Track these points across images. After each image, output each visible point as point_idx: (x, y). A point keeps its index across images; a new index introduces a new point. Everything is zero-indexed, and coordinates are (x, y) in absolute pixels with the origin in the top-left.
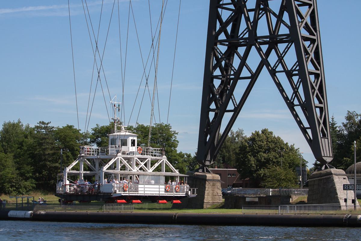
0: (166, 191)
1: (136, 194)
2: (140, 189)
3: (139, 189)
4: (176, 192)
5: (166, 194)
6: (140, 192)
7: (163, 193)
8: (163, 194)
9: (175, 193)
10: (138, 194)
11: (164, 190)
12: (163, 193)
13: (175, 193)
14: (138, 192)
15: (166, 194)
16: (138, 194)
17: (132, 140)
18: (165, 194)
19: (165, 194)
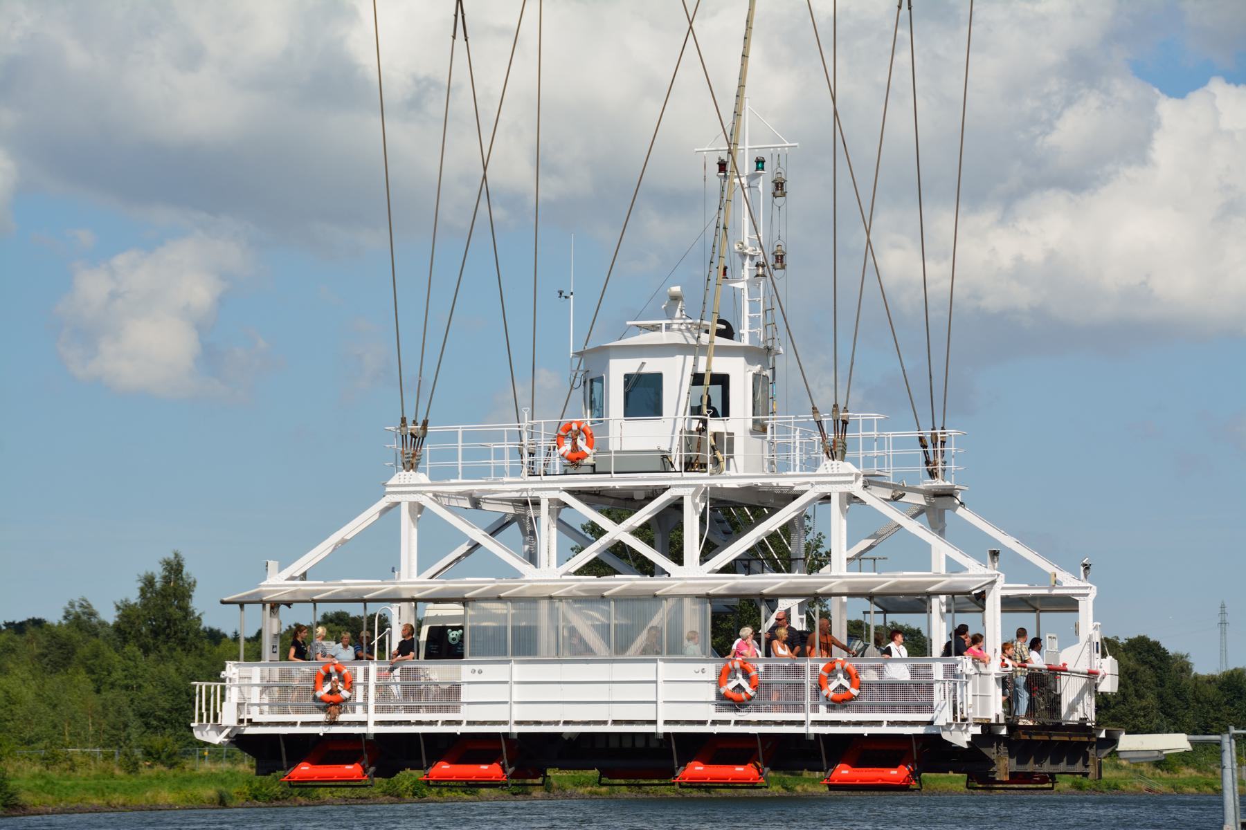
0: (729, 702)
1: (408, 723)
2: (466, 694)
4: (834, 705)
5: (727, 722)
6: (466, 714)
7: (710, 713)
8: (703, 723)
9: (823, 714)
10: (459, 723)
12: (710, 713)
13: (823, 714)
16: (459, 723)
17: (628, 377)
18: (714, 723)
19: (714, 723)
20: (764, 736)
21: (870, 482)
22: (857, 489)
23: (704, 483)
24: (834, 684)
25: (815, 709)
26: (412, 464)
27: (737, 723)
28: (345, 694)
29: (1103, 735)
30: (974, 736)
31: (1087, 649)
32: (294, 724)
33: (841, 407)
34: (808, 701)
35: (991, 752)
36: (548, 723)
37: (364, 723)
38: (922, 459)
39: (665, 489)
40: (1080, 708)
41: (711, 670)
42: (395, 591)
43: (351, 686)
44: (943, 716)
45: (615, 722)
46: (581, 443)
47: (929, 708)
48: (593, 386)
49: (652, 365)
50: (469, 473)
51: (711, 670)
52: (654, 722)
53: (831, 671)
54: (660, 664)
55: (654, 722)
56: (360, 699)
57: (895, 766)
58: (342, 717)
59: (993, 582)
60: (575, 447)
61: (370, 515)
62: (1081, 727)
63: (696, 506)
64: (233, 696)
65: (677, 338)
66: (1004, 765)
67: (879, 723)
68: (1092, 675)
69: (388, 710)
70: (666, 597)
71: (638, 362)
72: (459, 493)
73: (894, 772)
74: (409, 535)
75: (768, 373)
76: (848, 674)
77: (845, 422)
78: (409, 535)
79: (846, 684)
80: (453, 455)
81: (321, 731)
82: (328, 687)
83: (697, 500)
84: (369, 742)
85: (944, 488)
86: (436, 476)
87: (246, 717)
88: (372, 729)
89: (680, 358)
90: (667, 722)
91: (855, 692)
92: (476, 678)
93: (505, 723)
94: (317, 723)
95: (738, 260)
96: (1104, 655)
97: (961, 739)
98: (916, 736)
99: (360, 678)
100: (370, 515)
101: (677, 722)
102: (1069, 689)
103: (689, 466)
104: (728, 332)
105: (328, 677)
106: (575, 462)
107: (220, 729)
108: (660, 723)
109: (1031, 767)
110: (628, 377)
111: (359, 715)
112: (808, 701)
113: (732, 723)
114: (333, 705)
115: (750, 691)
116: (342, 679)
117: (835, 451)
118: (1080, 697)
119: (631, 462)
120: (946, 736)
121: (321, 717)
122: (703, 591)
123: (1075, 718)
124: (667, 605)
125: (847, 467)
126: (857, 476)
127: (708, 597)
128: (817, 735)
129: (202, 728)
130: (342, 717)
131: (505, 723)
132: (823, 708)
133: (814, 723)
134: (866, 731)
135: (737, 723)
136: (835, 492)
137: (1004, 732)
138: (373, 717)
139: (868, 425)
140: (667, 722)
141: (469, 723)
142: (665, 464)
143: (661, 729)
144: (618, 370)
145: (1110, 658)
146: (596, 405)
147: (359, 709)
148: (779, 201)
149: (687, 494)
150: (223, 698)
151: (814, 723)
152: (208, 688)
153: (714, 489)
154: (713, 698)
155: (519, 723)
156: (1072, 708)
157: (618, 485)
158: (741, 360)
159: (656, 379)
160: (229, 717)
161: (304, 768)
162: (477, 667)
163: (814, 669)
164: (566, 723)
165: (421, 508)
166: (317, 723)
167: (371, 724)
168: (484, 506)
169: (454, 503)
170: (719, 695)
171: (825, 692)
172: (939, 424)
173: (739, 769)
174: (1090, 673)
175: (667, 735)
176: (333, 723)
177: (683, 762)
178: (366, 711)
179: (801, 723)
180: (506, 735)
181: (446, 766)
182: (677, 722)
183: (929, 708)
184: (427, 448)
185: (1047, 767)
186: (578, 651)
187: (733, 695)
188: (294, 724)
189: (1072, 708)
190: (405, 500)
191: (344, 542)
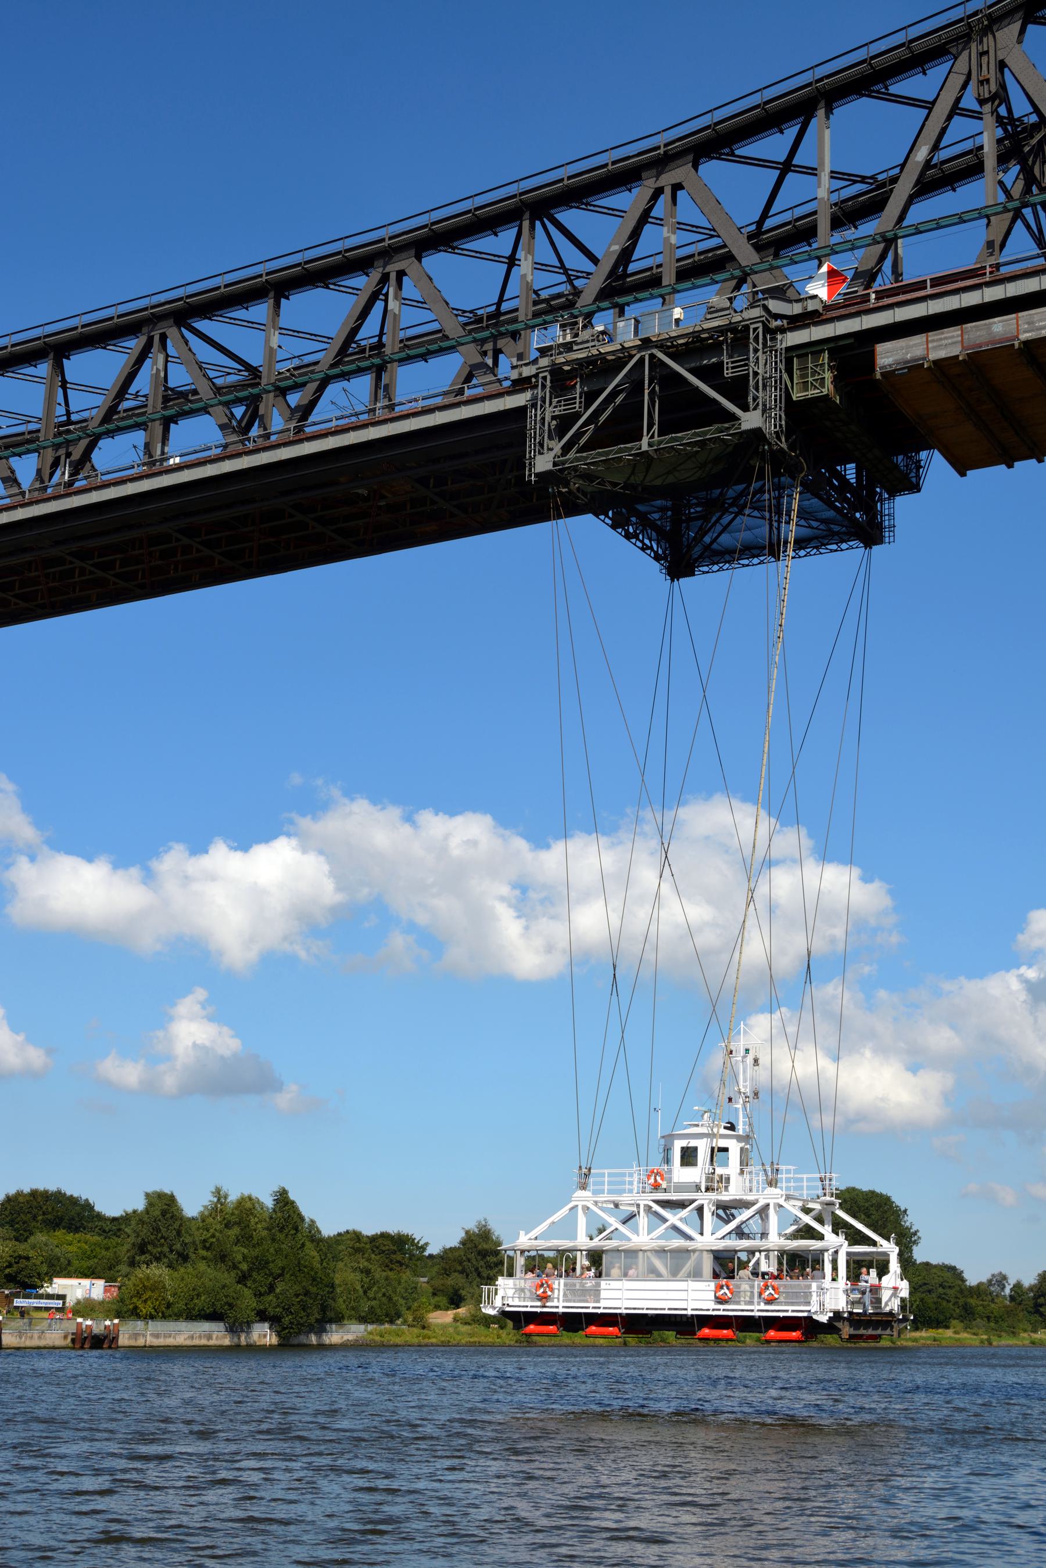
0: (720, 1301)
2: (603, 1294)
3: (602, 1292)
5: (719, 1310)
6: (603, 1303)
7: (712, 1305)
8: (708, 1310)
9: (763, 1306)
10: (599, 1308)
11: (712, 1296)
12: (712, 1305)
13: (763, 1306)
14: (598, 1301)
15: (719, 1310)
16: (599, 1308)
17: (683, 1148)
18: (713, 1310)
19: (713, 1310)
20: (736, 1316)
21: (788, 1198)
22: (782, 1201)
23: (713, 1198)
24: (767, 1292)
25: (759, 1304)
26: (584, 1187)
27: (724, 1310)
28: (549, 1293)
29: (901, 1317)
30: (830, 1317)
31: (894, 1277)
32: (527, 1306)
33: (775, 1163)
34: (756, 1299)
35: (839, 1325)
36: (639, 1309)
37: (557, 1307)
38: (821, 1187)
39: (696, 1200)
40: (889, 1304)
41: (712, 1285)
42: (574, 1246)
43: (552, 1290)
44: (814, 1307)
45: (669, 1309)
46: (658, 1178)
47: (808, 1303)
48: (667, 1150)
49: (693, 1143)
50: (610, 1192)
51: (712, 1285)
52: (686, 1309)
53: (766, 1287)
54: (690, 1282)
55: (686, 1309)
56: (556, 1295)
57: (794, 1331)
58: (548, 1304)
59: (842, 1245)
60: (656, 1180)
61: (564, 1211)
62: (891, 1314)
63: (710, 1209)
64: (501, 1293)
65: (704, 1130)
66: (847, 1330)
67: (787, 1311)
68: (895, 1289)
69: (567, 1301)
70: (694, 1251)
71: (687, 1141)
72: (608, 1201)
73: (794, 1334)
74: (582, 1220)
75: (748, 1146)
76: (774, 1289)
77: (777, 1170)
78: (582, 1220)
79: (773, 1292)
80: (603, 1184)
81: (539, 1310)
82: (542, 1290)
83: (711, 1206)
84: (559, 1316)
85: (830, 1201)
86: (595, 1193)
87: (506, 1302)
88: (561, 1310)
89: (705, 1139)
90: (692, 1310)
91: (776, 1296)
92: (608, 1287)
93: (620, 1308)
94: (537, 1307)
95: (738, 1095)
96: (902, 1280)
97: (824, 1319)
98: (804, 1317)
99: (556, 1286)
100: (564, 1211)
101: (697, 1310)
102: (885, 1296)
103: (707, 1189)
104: (732, 1127)
105: (542, 1285)
106: (656, 1187)
107: (494, 1308)
108: (689, 1310)
109: (862, 1332)
110: (683, 1148)
111: (555, 1303)
112: (756, 1299)
113: (722, 1310)
114: (544, 1298)
115: (729, 1295)
116: (549, 1286)
117: (772, 1183)
118: (890, 1299)
119: (681, 1188)
120: (815, 1317)
121: (539, 1304)
122: (709, 1248)
123: (888, 1309)
124: (697, 1254)
125: (777, 1191)
126: (782, 1196)
127: (712, 1251)
128: (759, 1317)
129: (485, 1307)
130: (548, 1304)
131: (620, 1308)
132: (762, 1304)
133: (758, 1311)
134: (781, 1314)
135: (724, 1310)
136: (772, 1202)
137: (846, 1315)
138: (561, 1304)
139: (788, 1172)
140: (692, 1310)
141: (604, 1308)
142: (698, 1188)
143: (690, 1312)
144: (678, 1145)
145: (905, 1281)
146: (667, 1160)
147: (556, 1300)
148: (756, 1068)
149: (705, 1203)
150: (496, 1294)
151: (758, 1311)
152: (489, 1289)
153: (718, 1200)
154: (713, 1298)
155: (626, 1308)
156: (886, 1304)
157: (674, 1198)
158: (735, 1141)
159: (695, 1149)
160: (498, 1302)
161: (532, 1327)
162: (608, 1282)
163: (759, 1285)
164: (647, 1309)
165: (588, 1208)
166: (537, 1307)
167: (560, 1307)
168: (621, 1207)
169: (605, 1205)
170: (716, 1297)
171: (763, 1296)
172: (828, 1170)
173: (725, 1332)
174: (894, 1288)
175: (692, 1315)
176: (544, 1306)
177: (700, 1329)
178: (558, 1301)
179: (752, 1311)
180: (620, 1314)
181: (594, 1328)
182: (697, 1310)
183: (808, 1303)
184: (591, 1180)
185: (879, 1332)
186: (654, 1274)
187: (722, 1297)
188: (527, 1306)
189: (886, 1304)
190: (580, 1204)
191: (553, 1223)
